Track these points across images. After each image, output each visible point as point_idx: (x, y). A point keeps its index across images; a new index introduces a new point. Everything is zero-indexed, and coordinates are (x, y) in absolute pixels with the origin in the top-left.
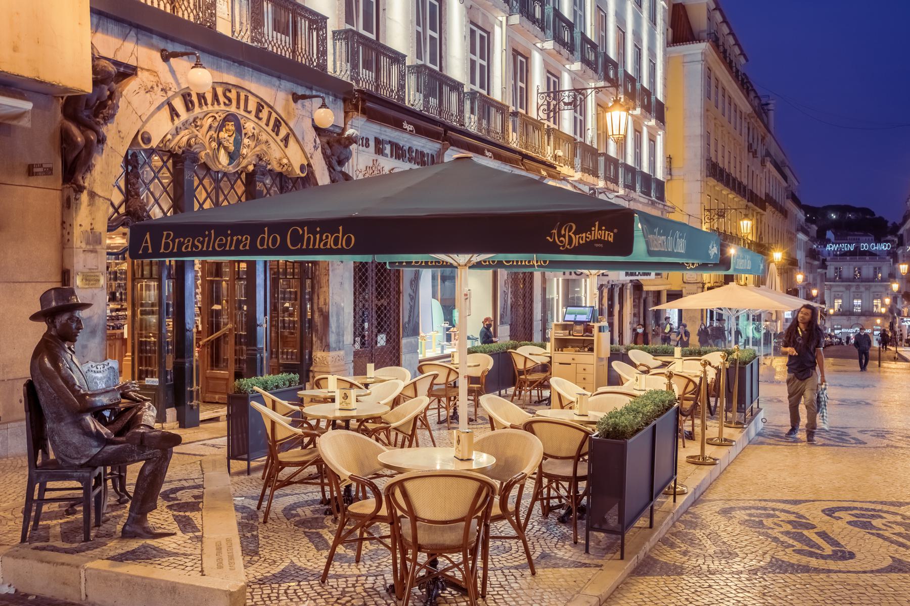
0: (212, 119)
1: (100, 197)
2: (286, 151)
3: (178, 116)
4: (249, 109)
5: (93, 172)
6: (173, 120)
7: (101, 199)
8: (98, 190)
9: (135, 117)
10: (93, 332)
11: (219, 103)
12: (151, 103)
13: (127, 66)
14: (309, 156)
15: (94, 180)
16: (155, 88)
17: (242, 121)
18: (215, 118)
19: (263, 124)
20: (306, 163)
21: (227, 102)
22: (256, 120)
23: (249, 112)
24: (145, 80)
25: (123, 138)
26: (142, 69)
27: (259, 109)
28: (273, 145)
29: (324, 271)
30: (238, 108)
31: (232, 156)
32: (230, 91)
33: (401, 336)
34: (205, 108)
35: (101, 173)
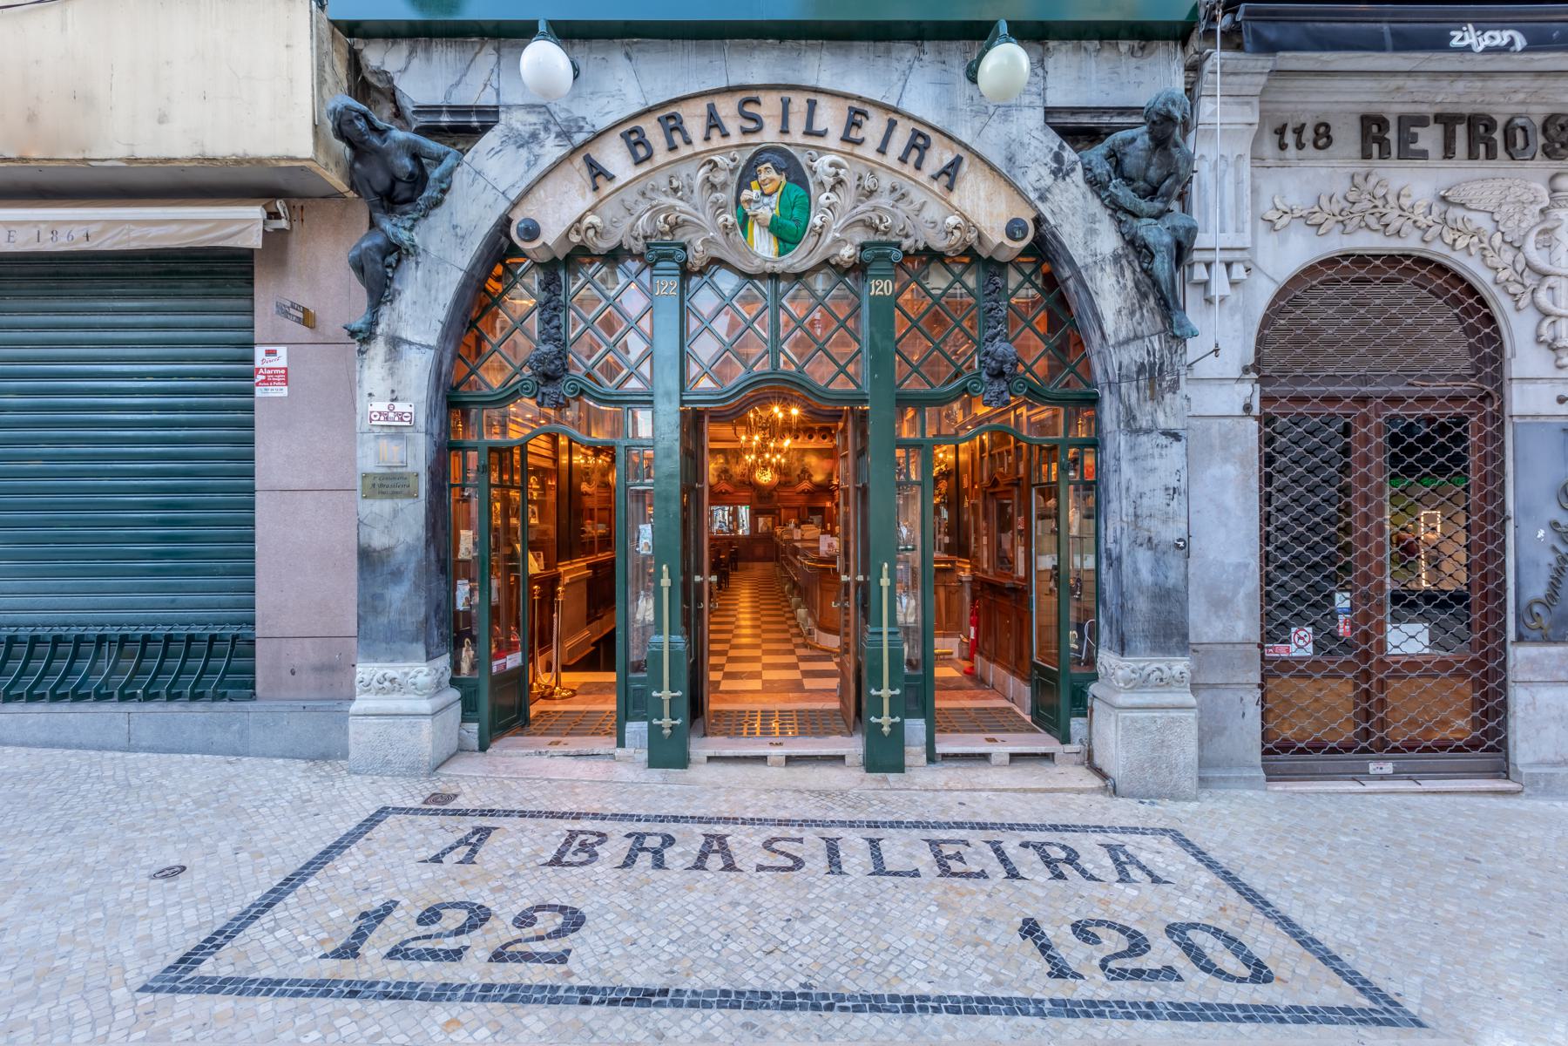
0: (707, 168)
1: (410, 343)
2: (954, 198)
3: (611, 178)
4: (818, 126)
5: (396, 304)
6: (596, 188)
7: (414, 347)
8: (407, 333)
9: (489, 196)
10: (396, 575)
11: (725, 135)
12: (529, 165)
13: (481, 111)
14: (1033, 196)
15: (400, 318)
16: (542, 135)
17: (803, 159)
18: (716, 165)
19: (868, 151)
20: (1028, 216)
21: (751, 125)
22: (848, 148)
23: (822, 134)
24: (518, 126)
25: (463, 237)
26: (509, 107)
27: (855, 119)
28: (917, 196)
29: (1112, 462)
30: (785, 131)
31: (786, 237)
32: (757, 102)
33: (1511, 635)
34: (685, 151)
35: (415, 303)
